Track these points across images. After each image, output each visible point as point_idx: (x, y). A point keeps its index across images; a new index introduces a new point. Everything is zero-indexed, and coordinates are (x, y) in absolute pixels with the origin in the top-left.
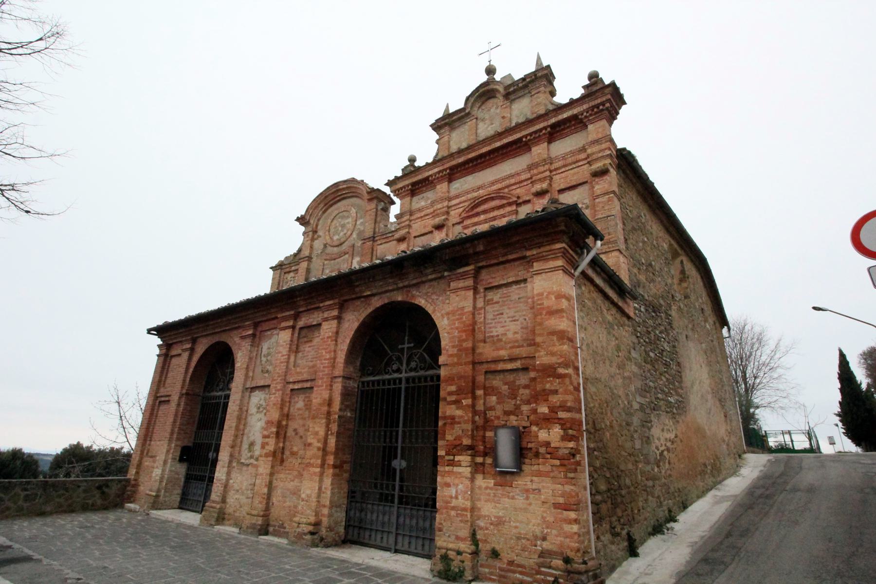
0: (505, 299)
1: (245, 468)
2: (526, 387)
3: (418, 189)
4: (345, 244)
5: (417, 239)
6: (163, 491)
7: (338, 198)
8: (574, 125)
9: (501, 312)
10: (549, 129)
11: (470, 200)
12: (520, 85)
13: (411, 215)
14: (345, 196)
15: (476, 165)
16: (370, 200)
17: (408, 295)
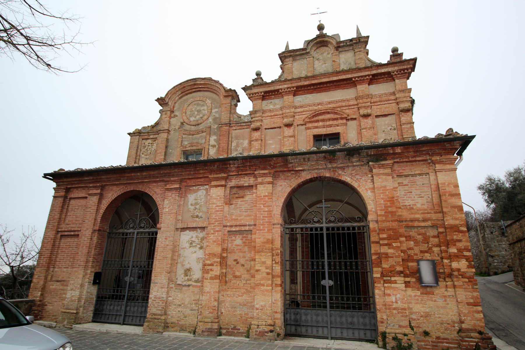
0: (412, 184)
1: (185, 288)
2: (434, 237)
3: (268, 96)
4: (202, 124)
5: (267, 130)
6: (81, 309)
7: (194, 90)
8: (386, 78)
9: (410, 191)
10: (371, 77)
11: (311, 111)
12: (348, 43)
13: (263, 113)
14: (201, 89)
15: (316, 88)
16: (225, 96)
17: (335, 174)
